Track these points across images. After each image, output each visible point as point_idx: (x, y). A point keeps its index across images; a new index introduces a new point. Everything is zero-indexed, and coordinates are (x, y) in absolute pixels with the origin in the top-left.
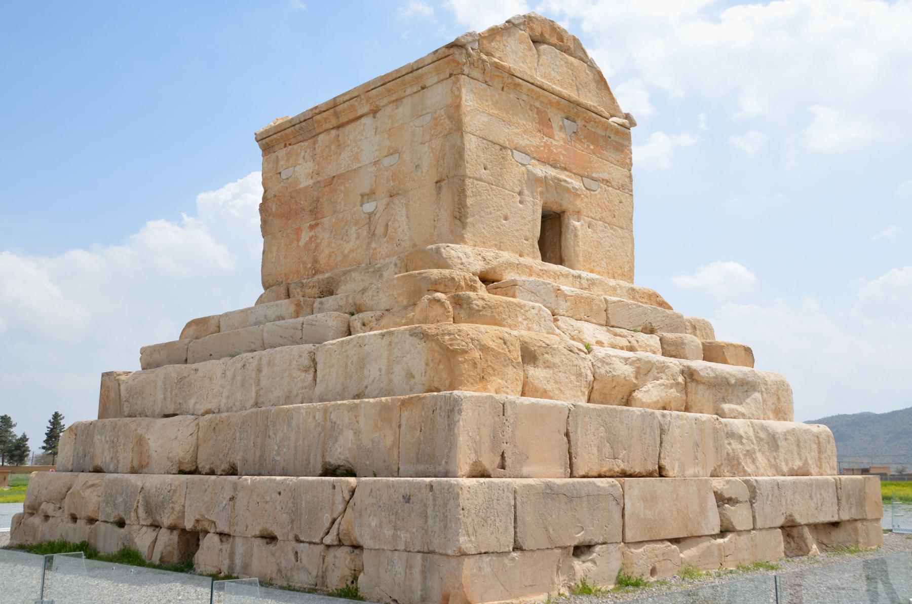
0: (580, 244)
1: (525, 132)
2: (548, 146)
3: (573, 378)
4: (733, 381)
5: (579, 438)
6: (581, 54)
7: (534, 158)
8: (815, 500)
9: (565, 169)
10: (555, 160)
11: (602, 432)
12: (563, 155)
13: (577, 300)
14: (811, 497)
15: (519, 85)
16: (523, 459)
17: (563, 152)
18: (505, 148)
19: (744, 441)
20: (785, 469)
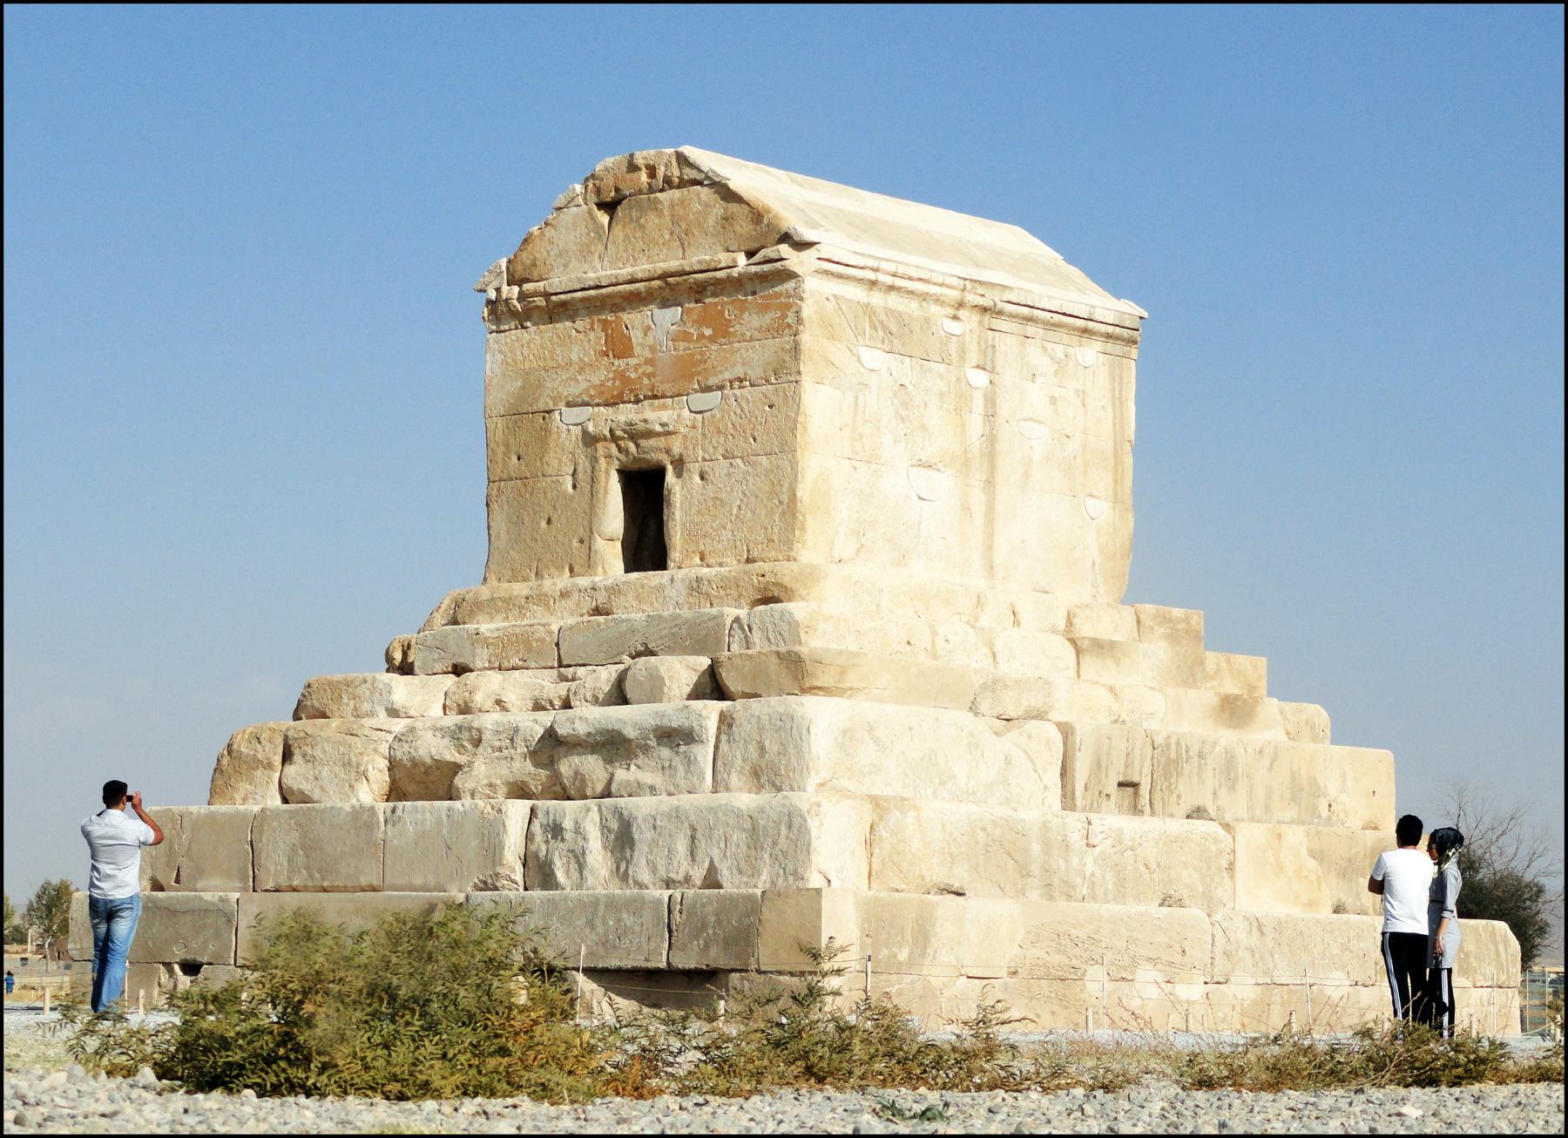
0: (678, 514)
1: (581, 370)
2: (621, 375)
3: (337, 769)
4: (631, 733)
5: (265, 848)
6: (690, 174)
7: (598, 405)
8: (600, 929)
9: (655, 397)
10: (631, 391)
11: (294, 837)
12: (649, 376)
13: (506, 642)
14: (591, 924)
15: (563, 304)
16: (199, 873)
17: (650, 369)
18: (549, 412)
19: (568, 836)
20: (645, 876)
